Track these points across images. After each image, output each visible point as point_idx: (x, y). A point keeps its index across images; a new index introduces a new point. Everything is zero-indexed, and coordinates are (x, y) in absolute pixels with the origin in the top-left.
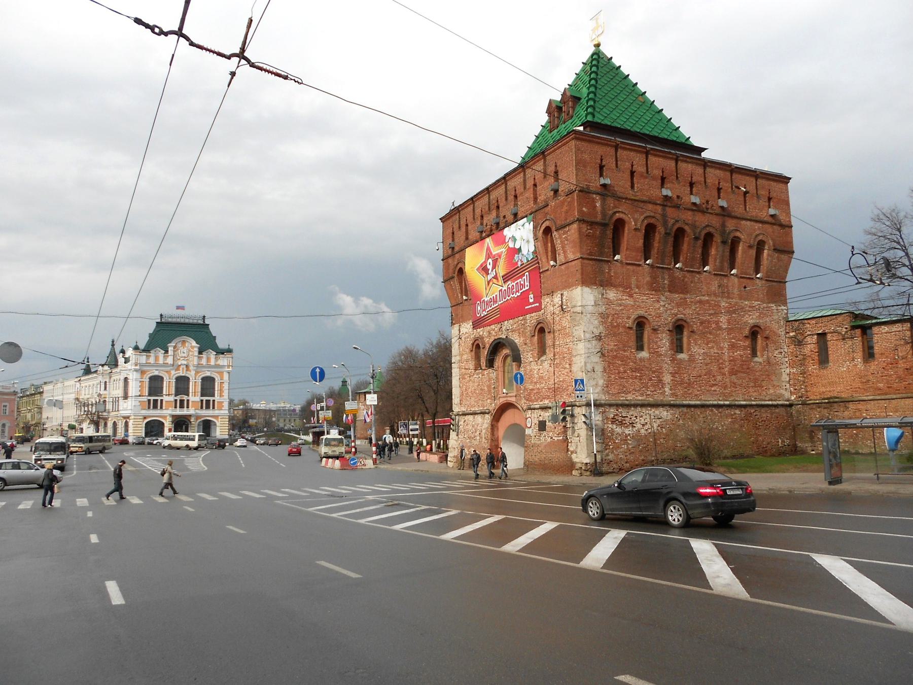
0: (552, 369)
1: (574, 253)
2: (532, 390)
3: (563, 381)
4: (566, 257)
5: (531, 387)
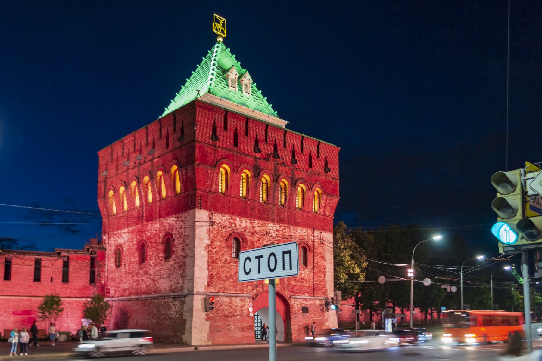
0: (312, 275)
1: (329, 213)
2: (295, 285)
3: (320, 284)
4: (324, 212)
5: (294, 283)
